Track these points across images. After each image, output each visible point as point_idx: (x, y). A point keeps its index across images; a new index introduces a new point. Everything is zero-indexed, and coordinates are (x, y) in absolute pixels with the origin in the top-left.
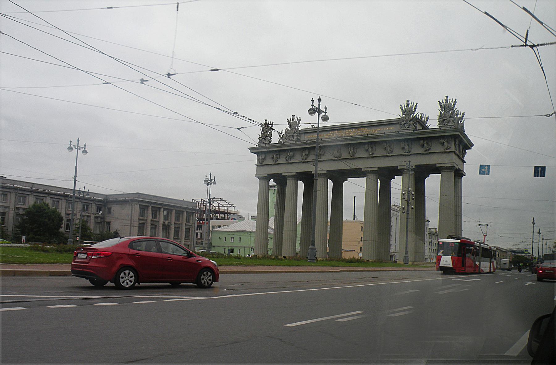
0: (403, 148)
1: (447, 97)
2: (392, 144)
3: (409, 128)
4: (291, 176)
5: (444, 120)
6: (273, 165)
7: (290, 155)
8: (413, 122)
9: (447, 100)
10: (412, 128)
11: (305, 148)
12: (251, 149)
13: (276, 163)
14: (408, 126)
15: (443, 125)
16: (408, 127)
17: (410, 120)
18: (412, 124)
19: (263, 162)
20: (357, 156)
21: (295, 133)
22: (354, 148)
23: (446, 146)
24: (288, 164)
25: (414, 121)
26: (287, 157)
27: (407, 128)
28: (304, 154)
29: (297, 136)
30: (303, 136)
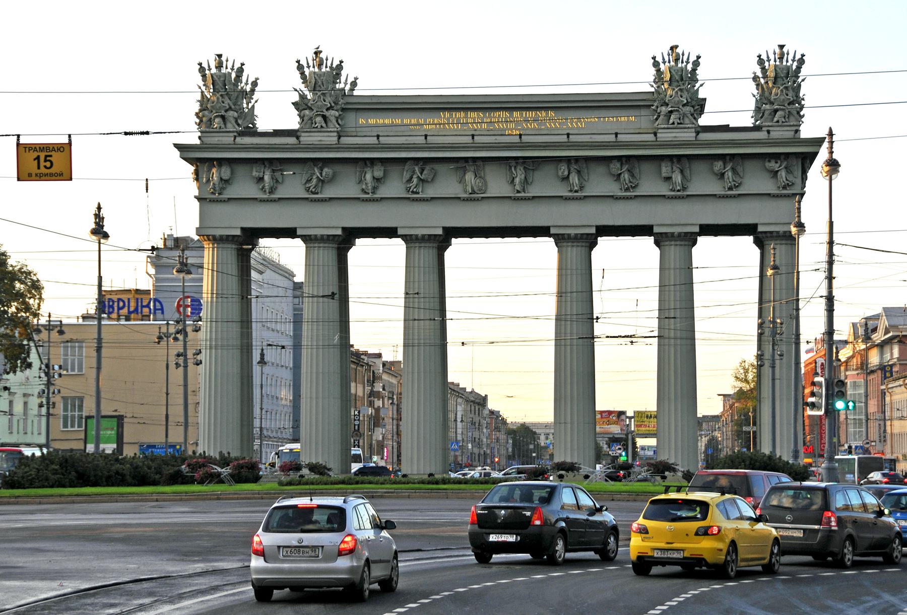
0: (668, 179)
1: (782, 47)
2: (636, 166)
3: (681, 124)
4: (432, 238)
6: (262, 201)
7: (321, 174)
8: (692, 110)
10: (691, 126)
11: (372, 161)
13: (273, 196)
19: (224, 189)
20: (533, 191)
22: (525, 168)
23: (785, 180)
24: (416, 200)
25: (693, 107)
26: (309, 181)
27: (678, 124)
28: (369, 177)
30: (351, 117)
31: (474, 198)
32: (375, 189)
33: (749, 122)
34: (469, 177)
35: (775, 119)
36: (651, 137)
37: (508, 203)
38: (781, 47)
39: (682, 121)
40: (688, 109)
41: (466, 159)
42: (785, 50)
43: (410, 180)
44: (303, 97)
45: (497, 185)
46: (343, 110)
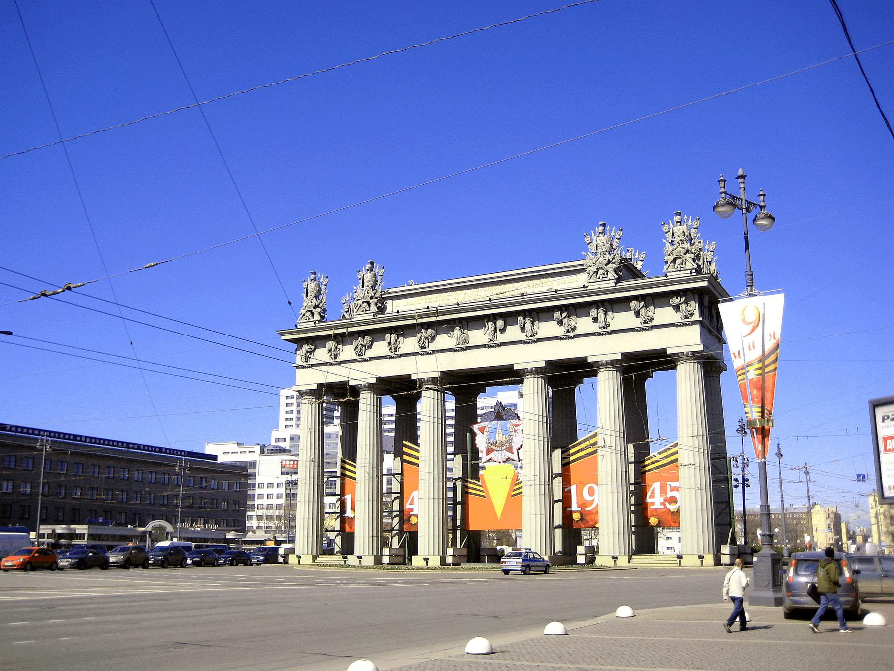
14: (604, 274)
15: (675, 270)
16: (604, 276)
17: (606, 262)
18: (610, 270)
21: (372, 298)
27: (603, 278)
34: (457, 331)
35: (676, 267)
39: (606, 276)
41: (454, 320)
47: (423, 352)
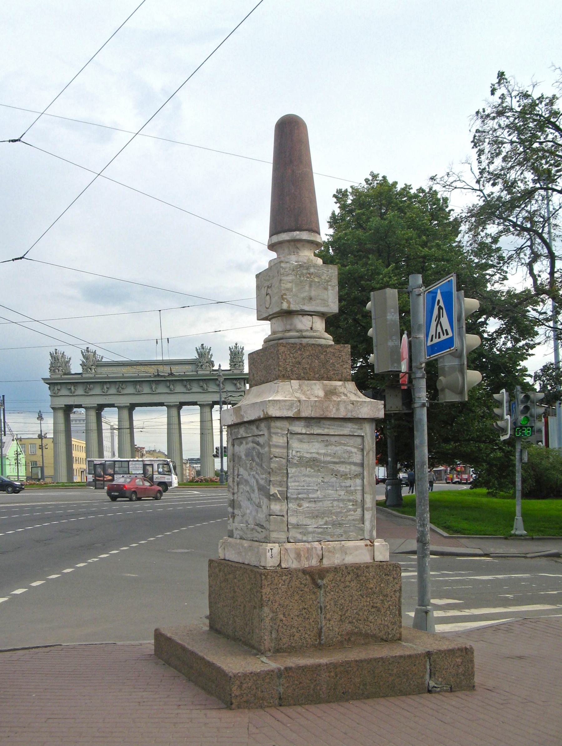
0: (202, 386)
1: (236, 344)
5: (235, 364)
6: (71, 396)
9: (236, 347)
12: (44, 379)
19: (58, 392)
26: (86, 389)
28: (105, 387)
29: (94, 369)
31: (139, 393)
32: (107, 391)
33: (229, 368)
36: (195, 373)
37: (150, 395)
38: (236, 344)
40: (208, 364)
42: (238, 345)
43: (118, 388)
44: (83, 362)
45: (146, 389)
46: (97, 366)
47: (119, 394)
